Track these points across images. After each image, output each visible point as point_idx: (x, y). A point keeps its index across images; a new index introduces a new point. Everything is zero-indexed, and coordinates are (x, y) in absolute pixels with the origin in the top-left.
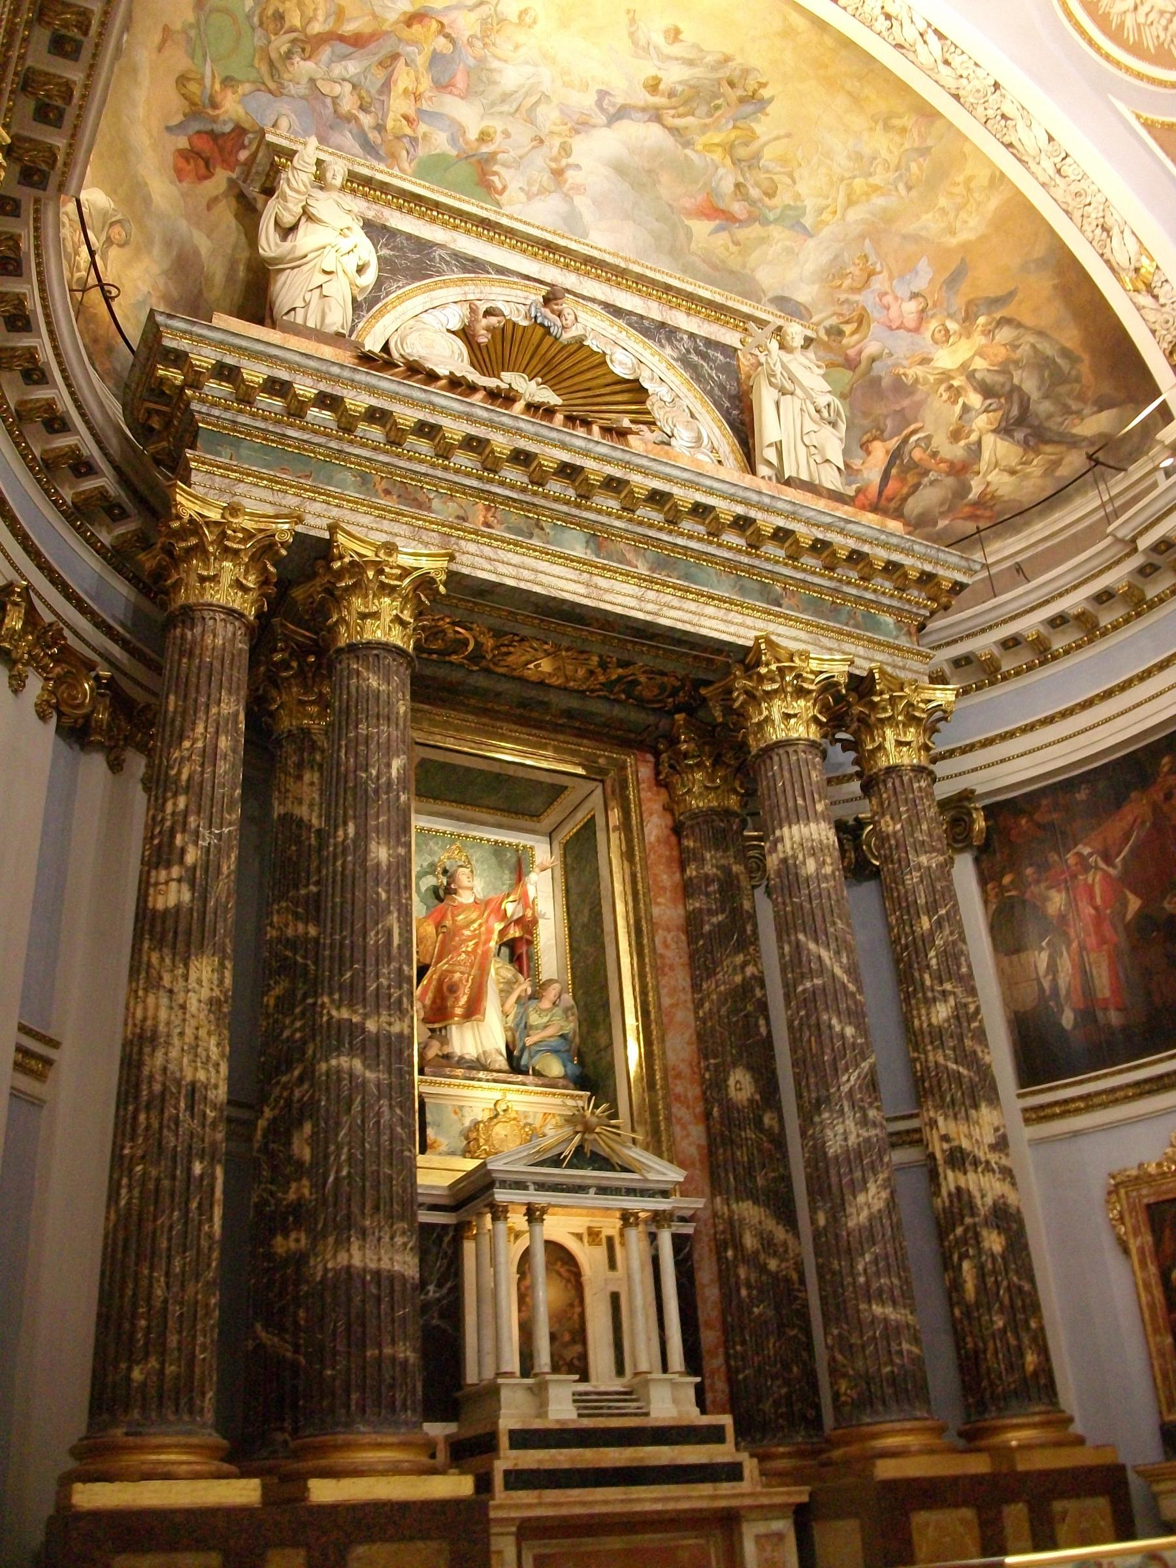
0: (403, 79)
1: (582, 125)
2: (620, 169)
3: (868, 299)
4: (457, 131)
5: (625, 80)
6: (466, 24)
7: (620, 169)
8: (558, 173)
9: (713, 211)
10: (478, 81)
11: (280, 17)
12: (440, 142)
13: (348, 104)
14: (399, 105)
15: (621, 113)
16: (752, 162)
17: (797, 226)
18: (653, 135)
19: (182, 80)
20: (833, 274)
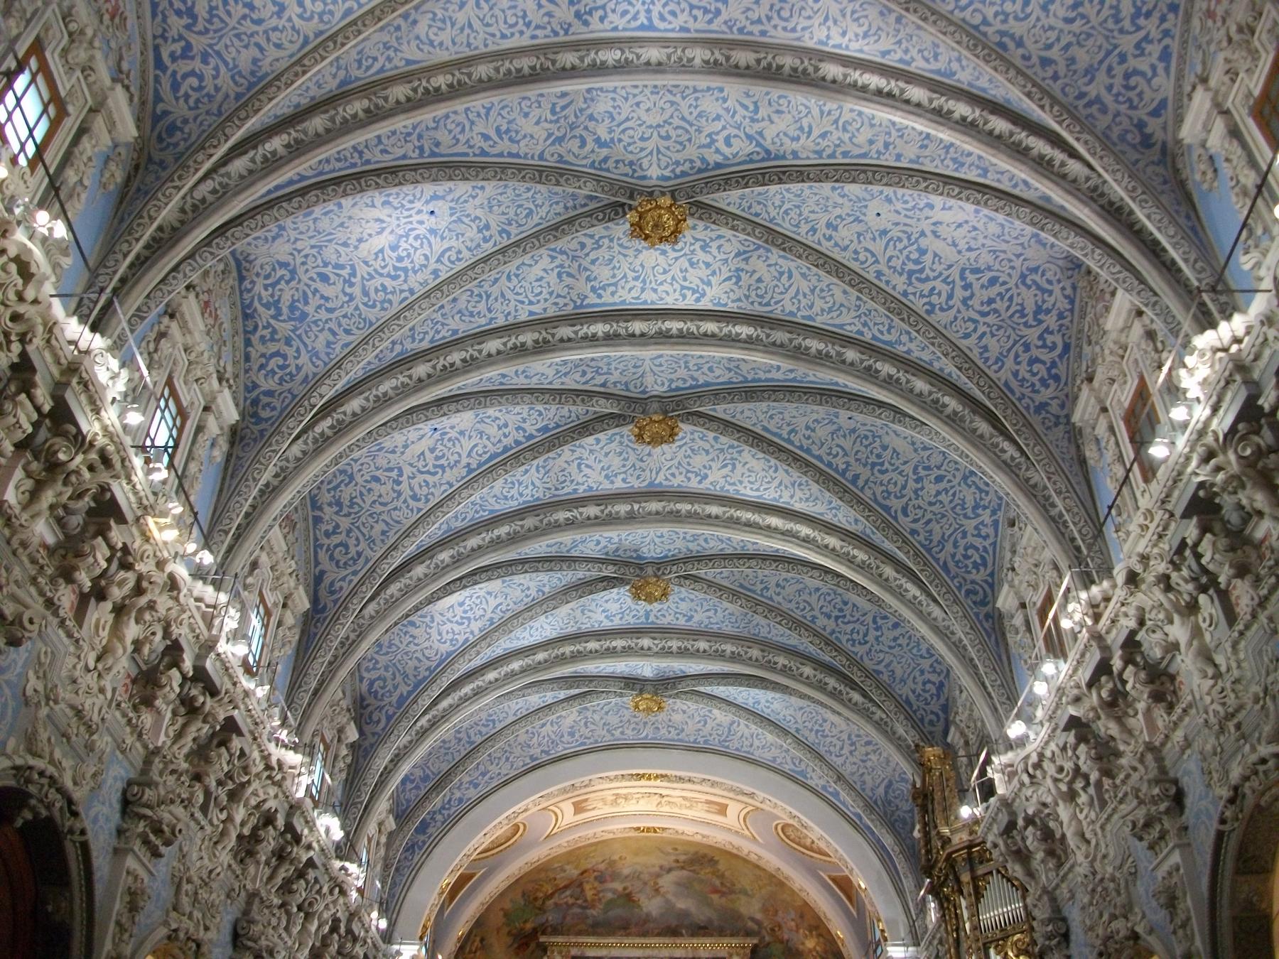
0: (587, 887)
1: (658, 876)
2: (678, 884)
3: (779, 919)
4: (614, 891)
5: (667, 861)
6: (602, 867)
7: (678, 884)
8: (657, 890)
9: (716, 891)
10: (615, 876)
11: (536, 899)
12: (610, 895)
13: (571, 901)
14: (589, 894)
15: (670, 870)
16: (722, 876)
17: (746, 894)
18: (685, 873)
19: (509, 933)
20: (765, 910)
